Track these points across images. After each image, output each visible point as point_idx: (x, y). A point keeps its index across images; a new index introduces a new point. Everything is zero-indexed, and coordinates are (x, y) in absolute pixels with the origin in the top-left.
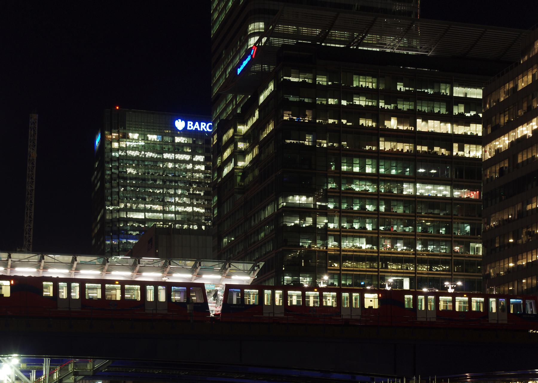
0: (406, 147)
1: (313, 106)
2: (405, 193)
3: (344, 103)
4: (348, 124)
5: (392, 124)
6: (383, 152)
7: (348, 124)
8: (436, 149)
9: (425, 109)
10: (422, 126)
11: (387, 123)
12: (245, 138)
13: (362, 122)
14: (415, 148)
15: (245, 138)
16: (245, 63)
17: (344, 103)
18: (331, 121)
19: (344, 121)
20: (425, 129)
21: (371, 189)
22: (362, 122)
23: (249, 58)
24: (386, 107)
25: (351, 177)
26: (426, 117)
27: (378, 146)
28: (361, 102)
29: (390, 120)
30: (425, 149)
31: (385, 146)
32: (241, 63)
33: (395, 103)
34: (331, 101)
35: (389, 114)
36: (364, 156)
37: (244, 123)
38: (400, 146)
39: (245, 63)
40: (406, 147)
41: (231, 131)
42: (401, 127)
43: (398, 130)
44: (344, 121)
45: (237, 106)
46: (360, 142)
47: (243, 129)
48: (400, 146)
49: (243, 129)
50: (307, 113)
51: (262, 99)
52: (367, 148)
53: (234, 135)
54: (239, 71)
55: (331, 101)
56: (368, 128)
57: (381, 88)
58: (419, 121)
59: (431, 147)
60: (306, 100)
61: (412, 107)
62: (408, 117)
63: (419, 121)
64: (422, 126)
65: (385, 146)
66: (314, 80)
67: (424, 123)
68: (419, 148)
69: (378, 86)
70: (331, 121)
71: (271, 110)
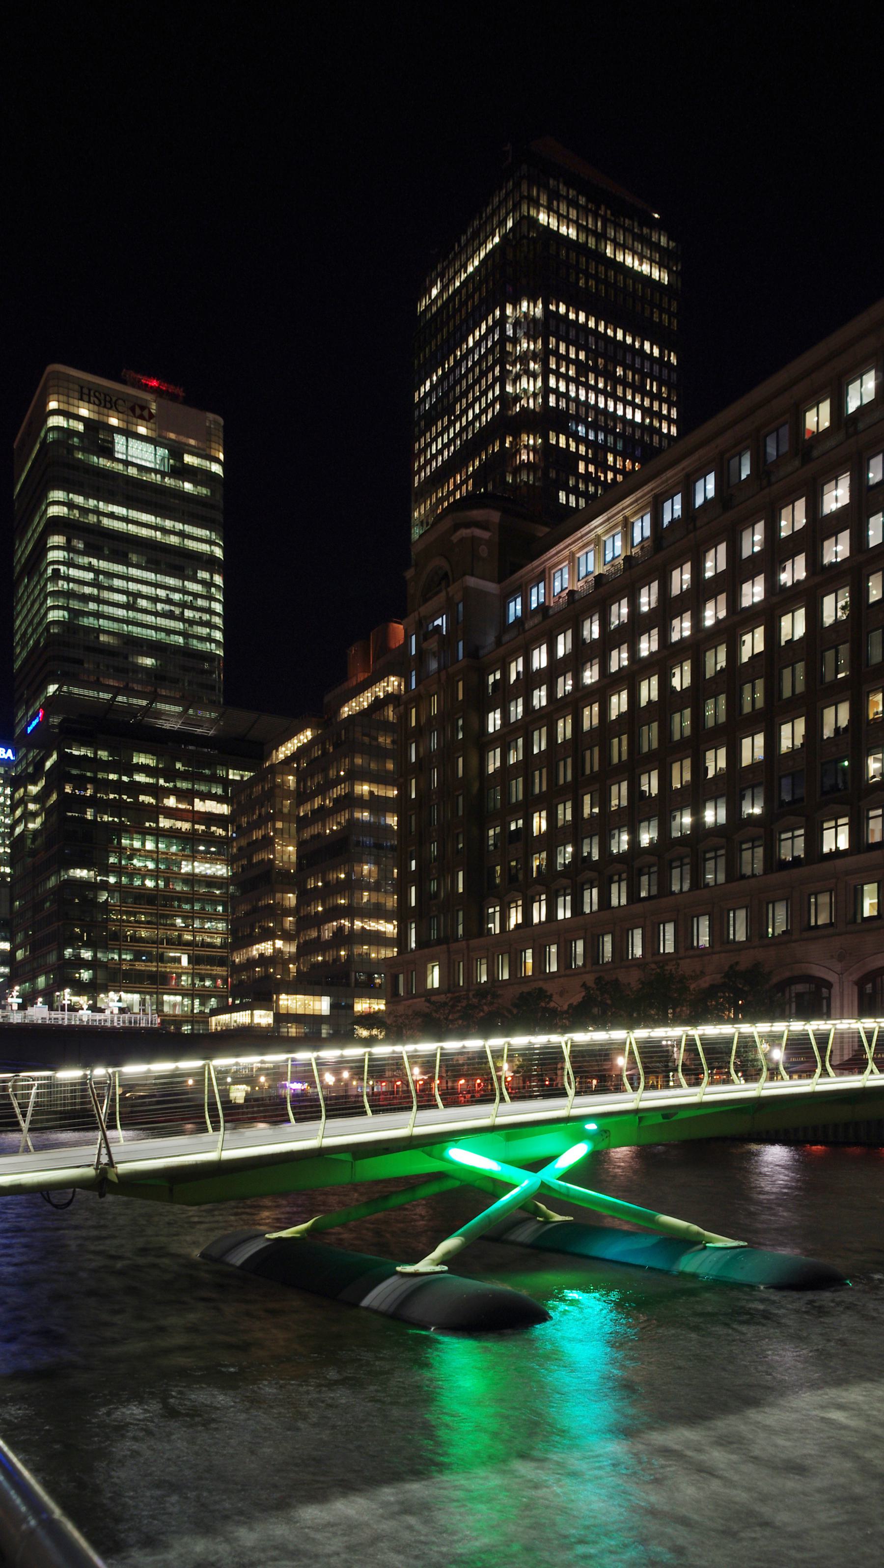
0: (185, 826)
1: (94, 781)
2: (183, 871)
3: (125, 779)
4: (128, 800)
5: (171, 802)
6: (163, 829)
7: (128, 800)
8: (213, 829)
9: (203, 788)
10: (200, 806)
11: (166, 801)
12: (36, 799)
13: (142, 798)
14: (193, 826)
15: (36, 799)
16: (34, 723)
17: (125, 779)
18: (111, 796)
19: (125, 797)
20: (202, 810)
21: (151, 865)
22: (142, 798)
23: (37, 720)
24: (167, 785)
25: (135, 853)
26: (204, 797)
27: (157, 822)
28: (141, 778)
29: (169, 798)
30: (203, 827)
31: (165, 823)
32: (29, 724)
33: (174, 782)
34: (112, 777)
35: (168, 792)
36: (144, 833)
37: (35, 783)
38: (179, 824)
39: (34, 723)
40: (185, 826)
41: (22, 790)
42: (181, 806)
43: (177, 809)
44: (125, 797)
45: (28, 765)
46: (140, 819)
47: (34, 789)
48: (179, 824)
49: (34, 789)
50: (89, 786)
51: (48, 764)
52: (147, 824)
53: (24, 795)
54: (29, 729)
55: (112, 777)
56: (150, 804)
57: (160, 766)
58: (197, 801)
59: (208, 827)
60: (89, 774)
61: (190, 786)
62: (187, 796)
63: (197, 801)
64: (200, 806)
65: (165, 823)
66: (96, 754)
67: (202, 803)
68: (197, 827)
69: (157, 763)
70: (111, 796)
71: (56, 778)
